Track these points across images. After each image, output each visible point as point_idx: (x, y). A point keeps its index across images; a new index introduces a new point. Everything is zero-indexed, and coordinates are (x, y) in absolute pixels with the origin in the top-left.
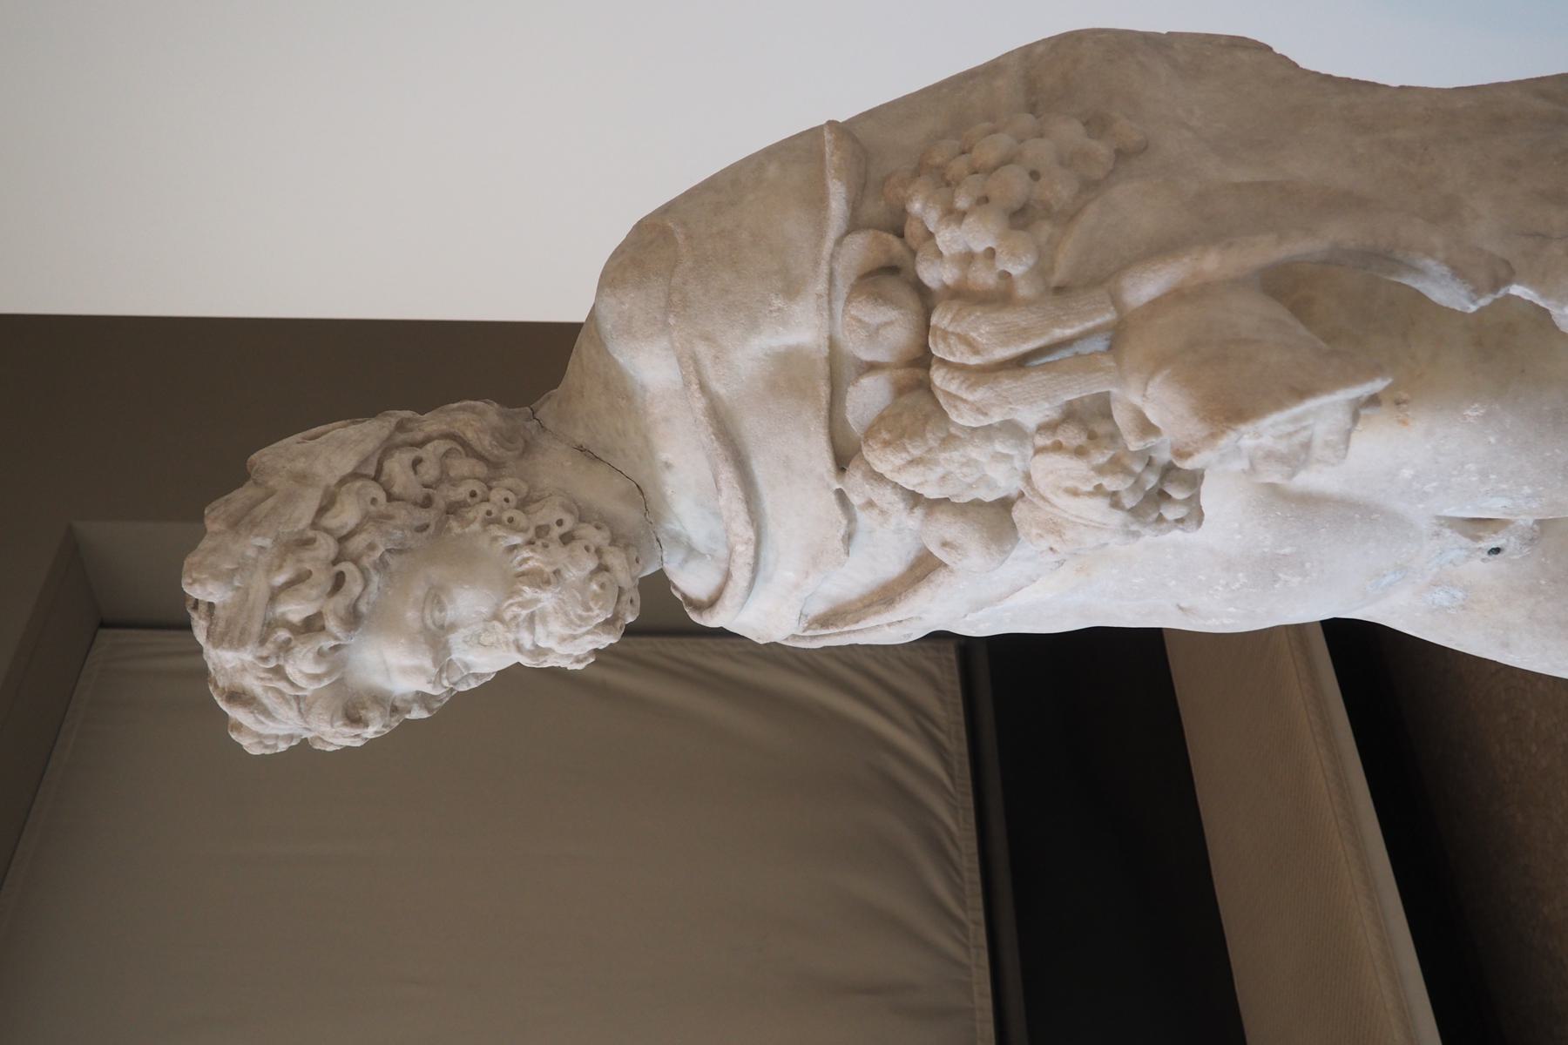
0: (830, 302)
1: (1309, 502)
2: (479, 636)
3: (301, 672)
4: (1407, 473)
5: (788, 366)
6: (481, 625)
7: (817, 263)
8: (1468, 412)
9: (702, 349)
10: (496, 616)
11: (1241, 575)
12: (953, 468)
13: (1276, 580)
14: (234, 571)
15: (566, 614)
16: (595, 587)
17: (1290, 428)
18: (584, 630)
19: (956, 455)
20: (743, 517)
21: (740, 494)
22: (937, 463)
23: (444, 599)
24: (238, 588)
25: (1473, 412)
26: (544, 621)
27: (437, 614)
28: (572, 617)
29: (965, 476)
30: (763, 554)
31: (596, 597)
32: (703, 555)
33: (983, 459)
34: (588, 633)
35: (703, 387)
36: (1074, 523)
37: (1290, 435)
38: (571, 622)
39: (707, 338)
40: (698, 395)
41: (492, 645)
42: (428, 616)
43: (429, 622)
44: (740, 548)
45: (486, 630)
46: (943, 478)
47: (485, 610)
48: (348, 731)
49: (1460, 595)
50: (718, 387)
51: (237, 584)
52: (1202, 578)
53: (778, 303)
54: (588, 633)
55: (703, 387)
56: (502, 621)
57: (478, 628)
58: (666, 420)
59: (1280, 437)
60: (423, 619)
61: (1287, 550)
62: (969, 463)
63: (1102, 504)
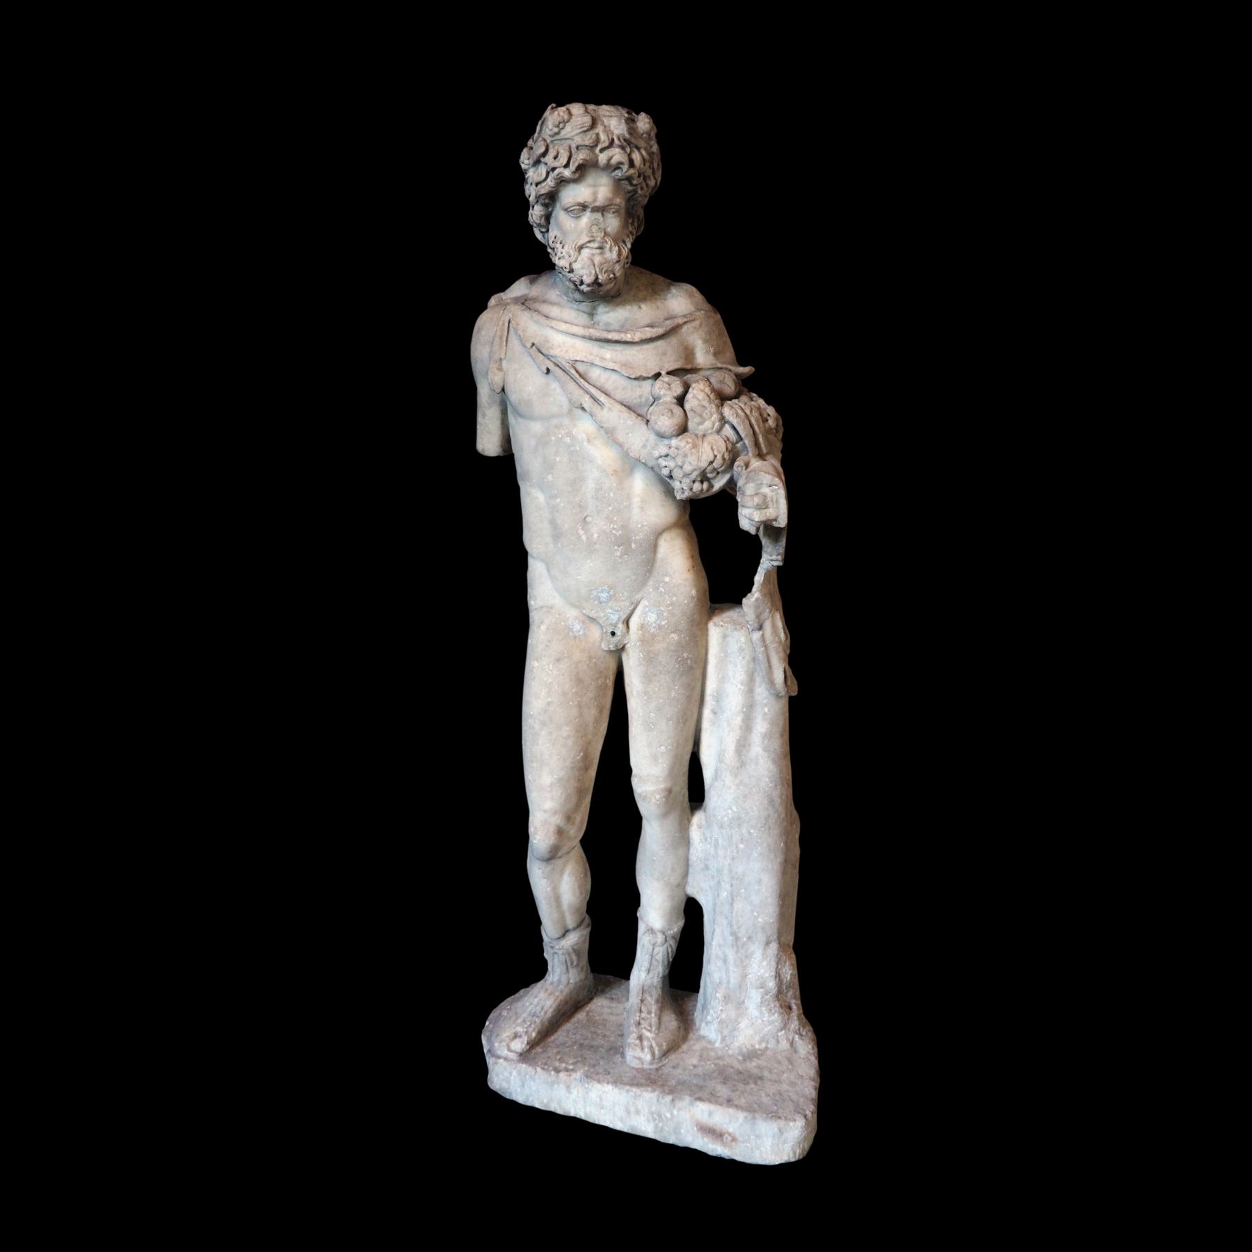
0: (714, 368)
1: (654, 547)
2: (597, 225)
3: (616, 154)
4: (667, 579)
5: (689, 353)
6: (603, 227)
7: (724, 363)
8: (694, 590)
9: (697, 323)
10: (606, 234)
11: (620, 532)
12: (709, 409)
13: (619, 546)
14: (649, 135)
15: (605, 263)
16: (612, 276)
17: (774, 500)
18: (598, 270)
19: (714, 410)
20: (644, 337)
21: (654, 336)
22: (710, 403)
23: (616, 214)
24: (642, 135)
25: (694, 592)
26: (602, 254)
27: (613, 210)
28: (605, 265)
29: (706, 413)
30: (618, 345)
31: (609, 276)
32: (592, 320)
33: (713, 419)
34: (596, 272)
35: (685, 323)
36: (699, 452)
37: (772, 501)
38: (601, 264)
39: (701, 324)
40: (684, 321)
41: (591, 230)
42: (616, 207)
43: (612, 207)
44: (629, 336)
45: (599, 229)
46: (704, 406)
47: (609, 229)
48: (576, 164)
49: (581, 633)
50: (685, 328)
51: (644, 135)
52: (615, 519)
53: (712, 350)
54: (596, 272)
55: (685, 323)
56: (604, 236)
57: (602, 226)
58: (658, 308)
59: (772, 498)
60: (615, 205)
61: (633, 546)
62: (712, 415)
63: (711, 458)
